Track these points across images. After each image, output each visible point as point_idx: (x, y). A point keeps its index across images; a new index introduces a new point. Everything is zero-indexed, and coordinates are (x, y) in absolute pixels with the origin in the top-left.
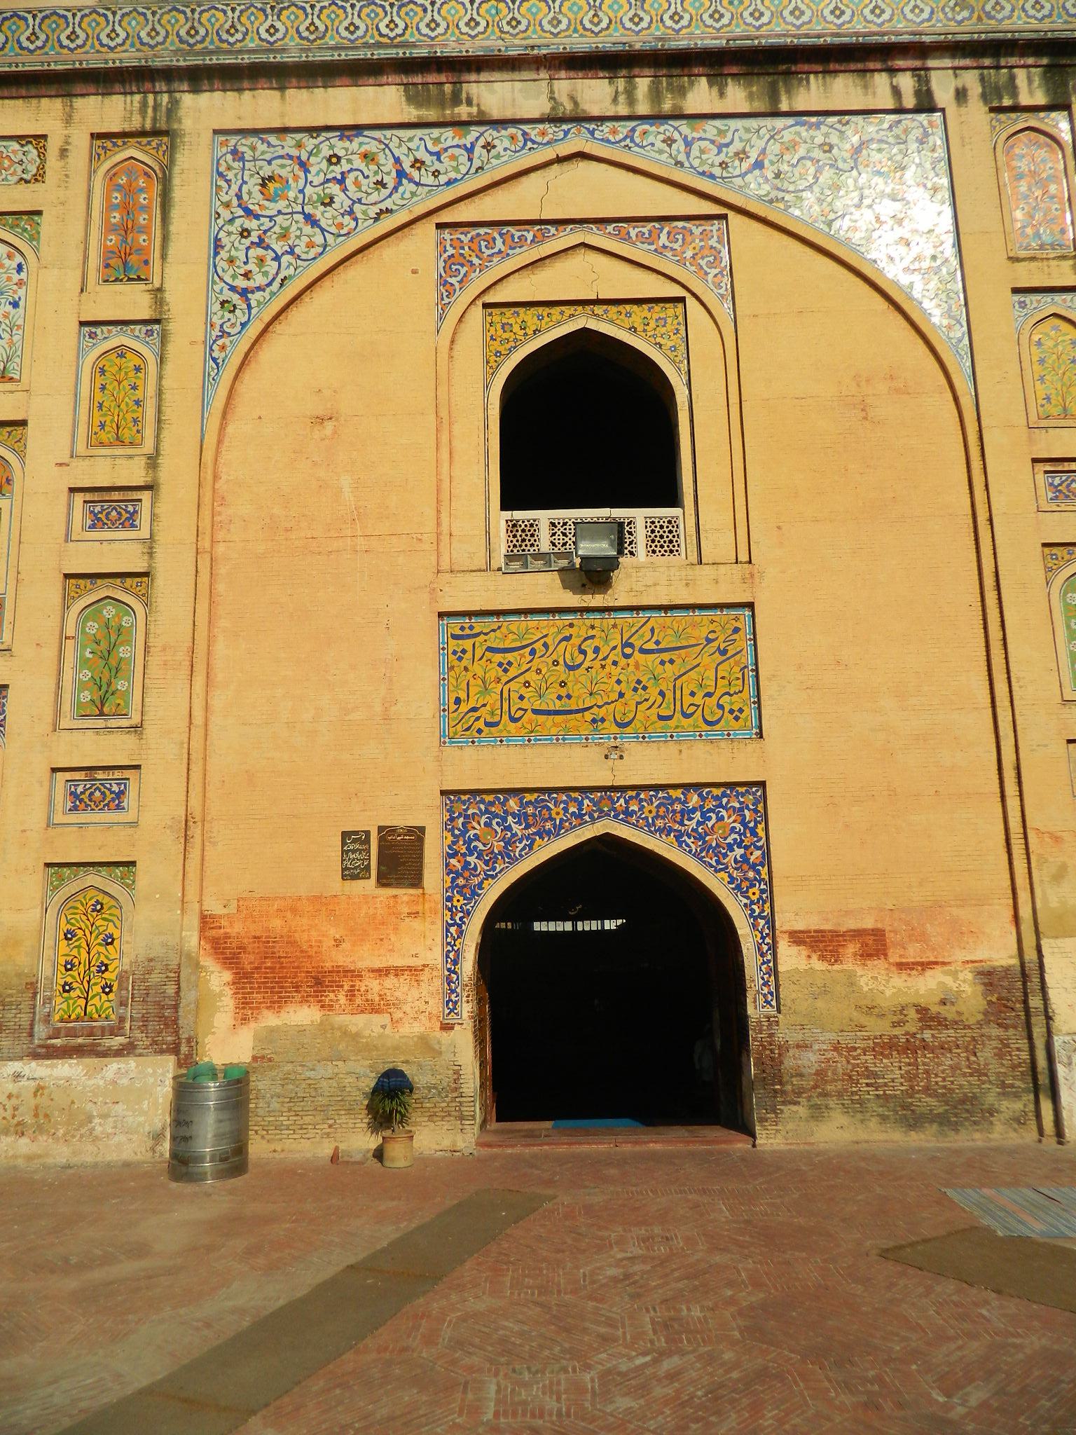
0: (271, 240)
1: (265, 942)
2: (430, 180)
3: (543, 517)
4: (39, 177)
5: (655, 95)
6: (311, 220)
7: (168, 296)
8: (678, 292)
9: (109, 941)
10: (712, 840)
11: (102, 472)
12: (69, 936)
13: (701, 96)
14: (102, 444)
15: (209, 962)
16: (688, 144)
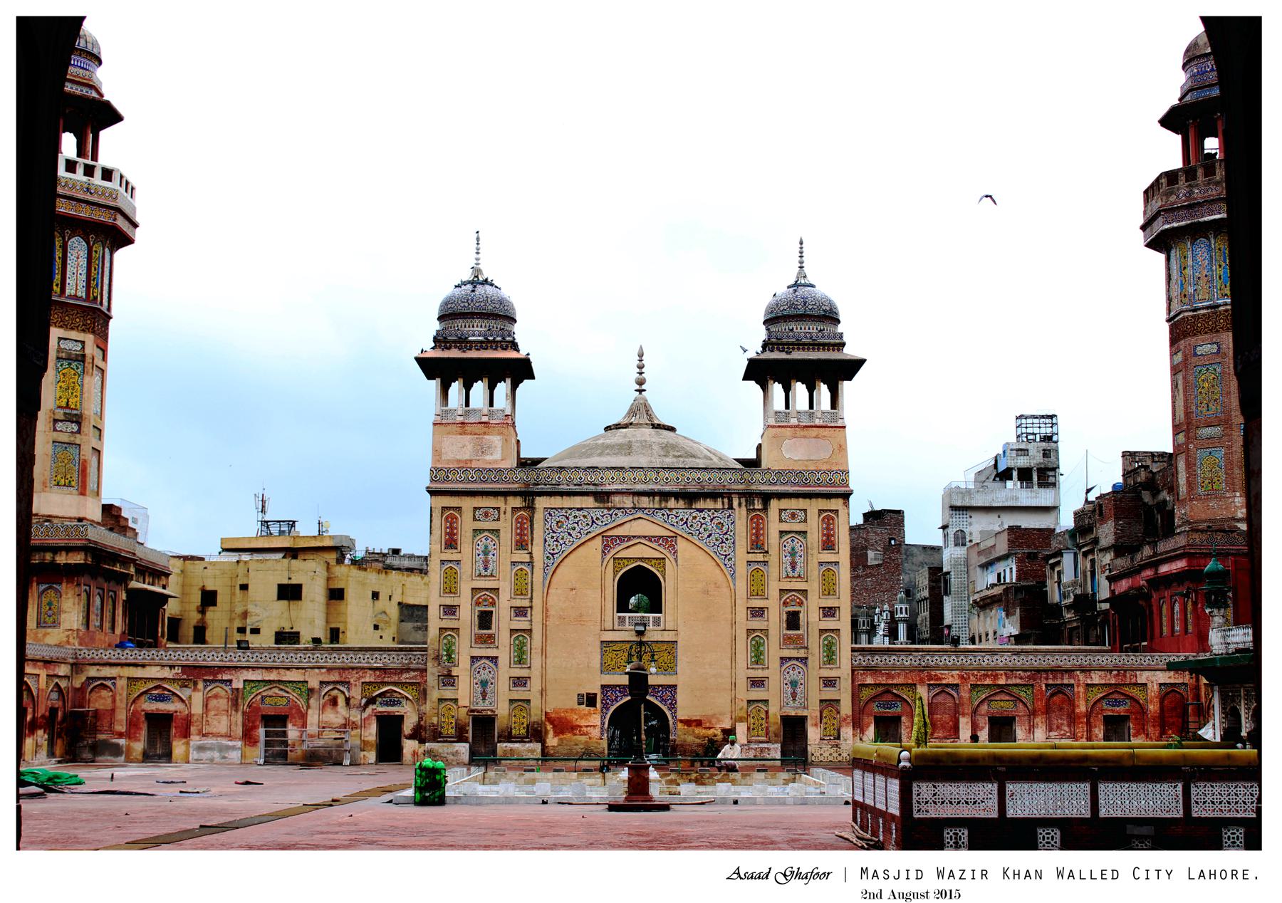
0: (559, 539)
1: (560, 719)
2: (600, 523)
3: (627, 615)
4: (498, 519)
5: (660, 501)
6: (570, 534)
7: (534, 555)
8: (664, 556)
9: (524, 717)
10: (664, 698)
11: (518, 603)
12: (515, 716)
13: (672, 503)
14: (517, 595)
15: (547, 723)
16: (668, 516)
